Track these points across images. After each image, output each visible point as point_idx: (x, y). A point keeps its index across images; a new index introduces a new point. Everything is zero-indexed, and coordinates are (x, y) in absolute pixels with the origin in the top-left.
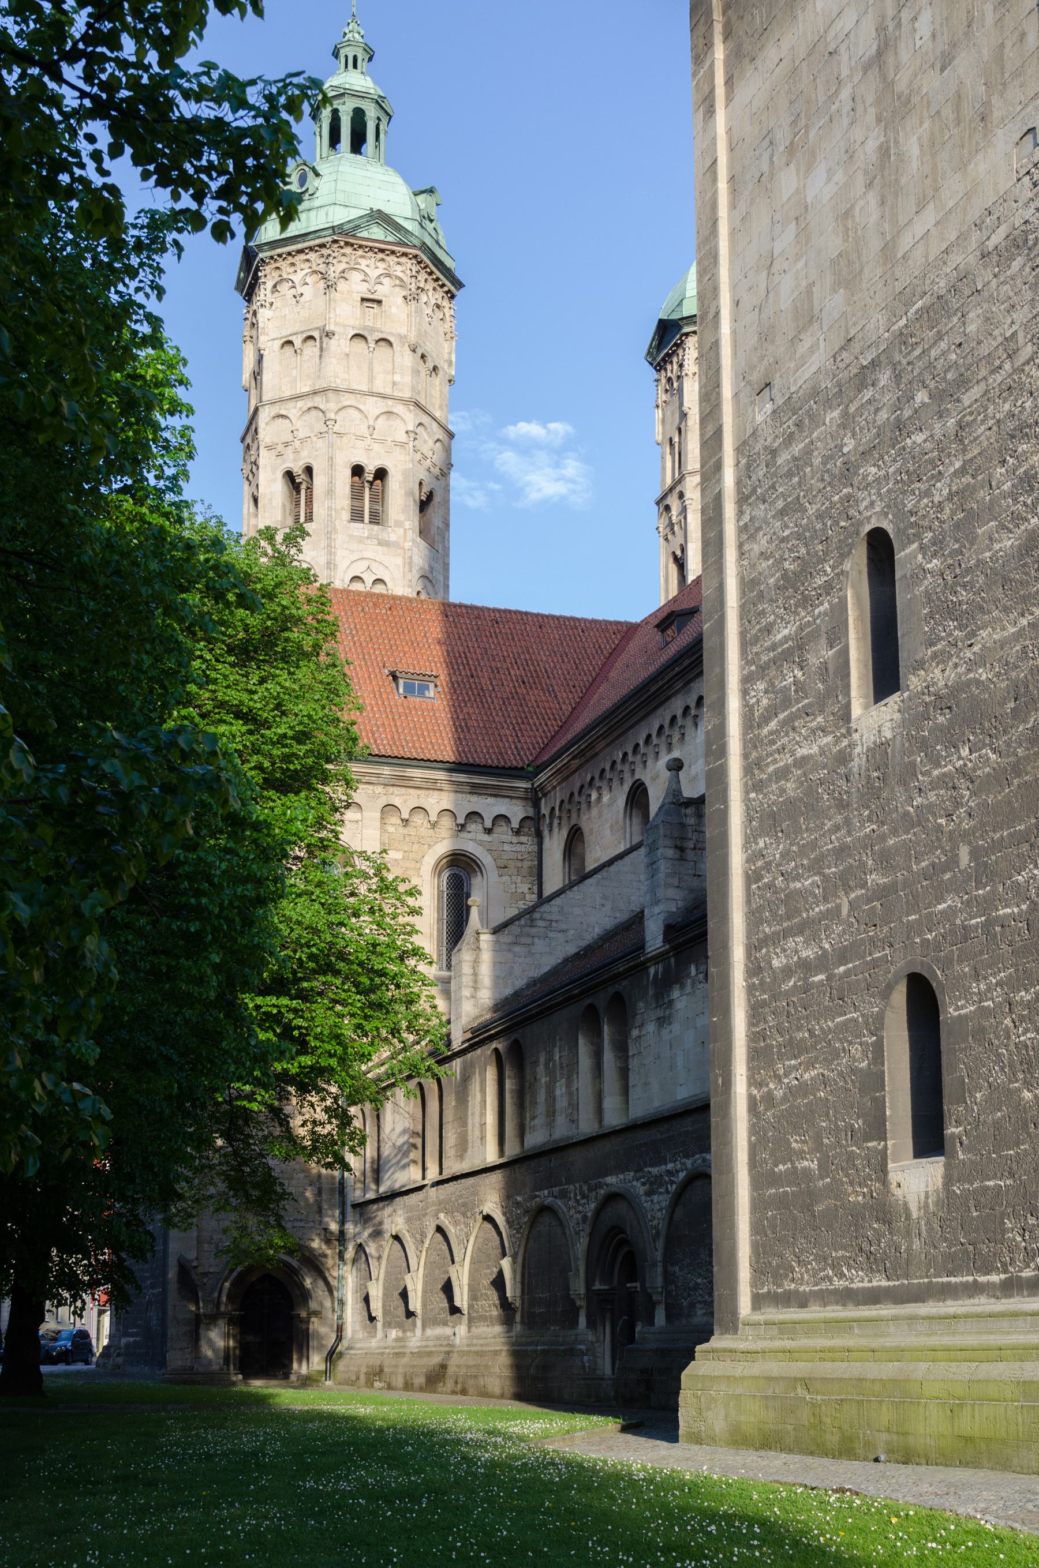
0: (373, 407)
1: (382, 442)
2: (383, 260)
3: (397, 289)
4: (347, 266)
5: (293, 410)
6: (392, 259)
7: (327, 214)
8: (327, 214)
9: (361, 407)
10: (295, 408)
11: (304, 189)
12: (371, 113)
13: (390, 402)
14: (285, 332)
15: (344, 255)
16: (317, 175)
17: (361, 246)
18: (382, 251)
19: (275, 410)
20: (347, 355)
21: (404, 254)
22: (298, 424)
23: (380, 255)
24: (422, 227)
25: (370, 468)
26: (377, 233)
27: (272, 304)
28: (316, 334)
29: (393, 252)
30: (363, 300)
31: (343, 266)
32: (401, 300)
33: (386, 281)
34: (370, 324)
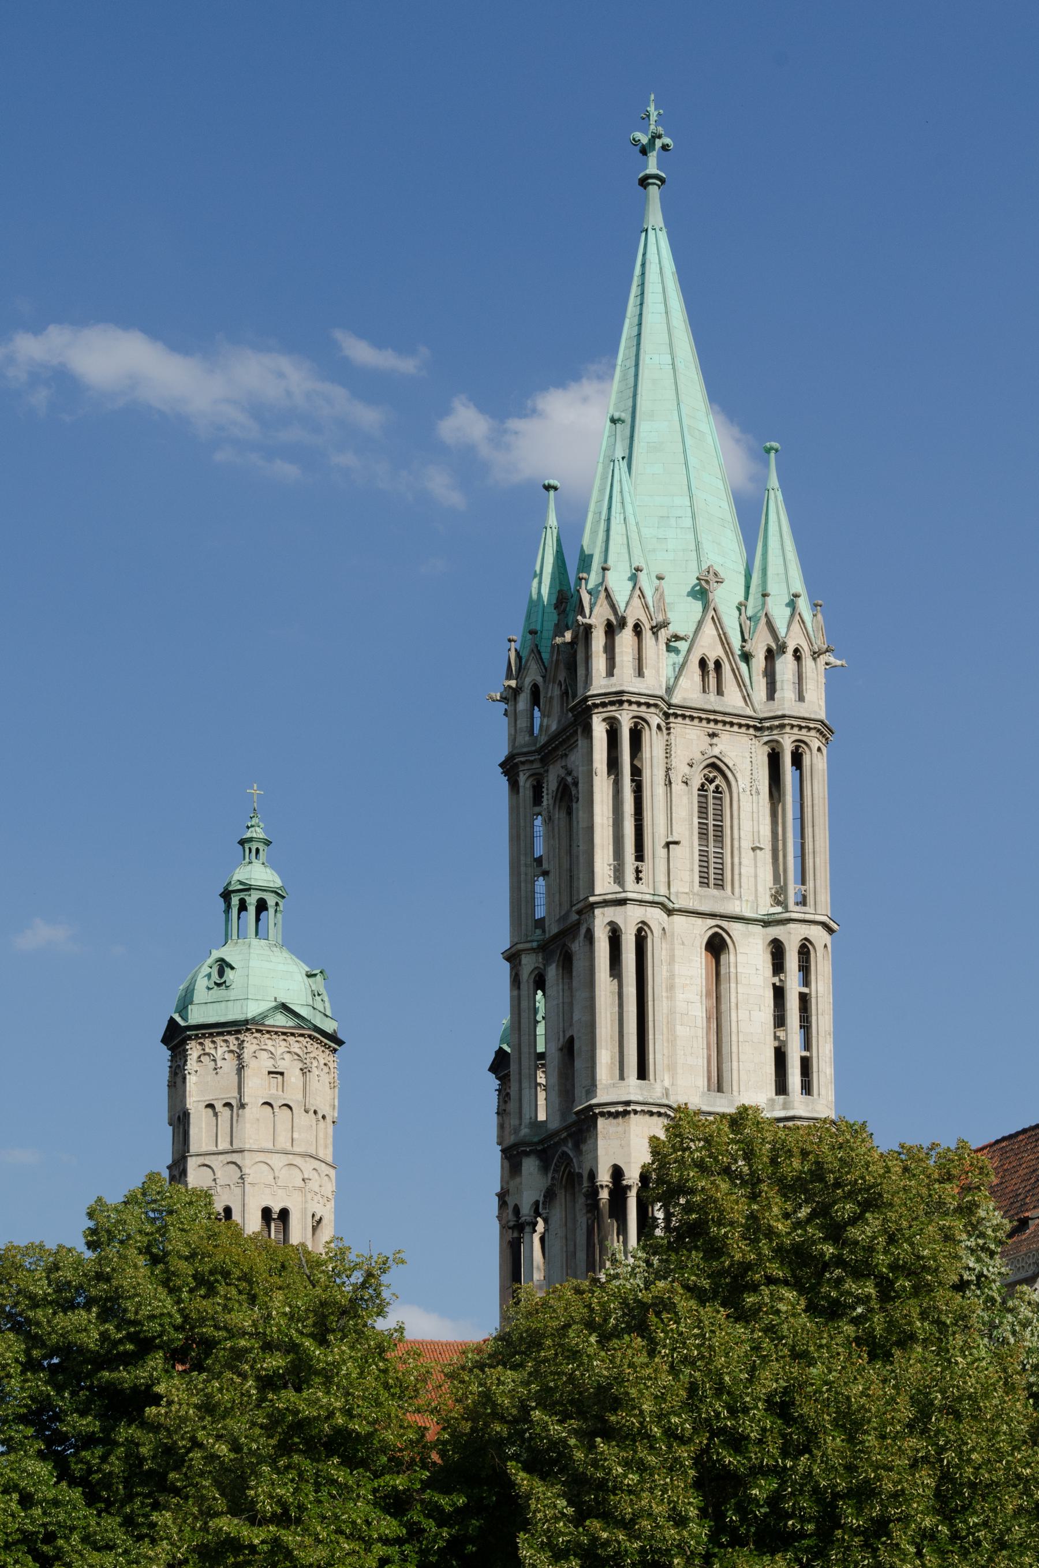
0: (277, 1161)
1: (285, 1187)
2: (284, 1040)
3: (296, 1062)
4: (258, 1047)
5: (215, 1162)
6: (291, 1039)
7: (242, 1007)
8: (242, 1007)
9: (269, 1162)
10: (217, 1160)
11: (222, 981)
12: (271, 900)
13: (291, 1156)
14: (208, 1098)
15: (255, 1038)
16: (232, 968)
17: (268, 1032)
18: (284, 1034)
19: (201, 1160)
20: (258, 1120)
21: (302, 1035)
22: (219, 1174)
23: (285, 1037)
24: (314, 1009)
25: (276, 1209)
26: (281, 1020)
27: (196, 1072)
28: (234, 1102)
29: (293, 1034)
30: (270, 1073)
31: (255, 1047)
32: (298, 1072)
33: (287, 1056)
34: (273, 1091)
